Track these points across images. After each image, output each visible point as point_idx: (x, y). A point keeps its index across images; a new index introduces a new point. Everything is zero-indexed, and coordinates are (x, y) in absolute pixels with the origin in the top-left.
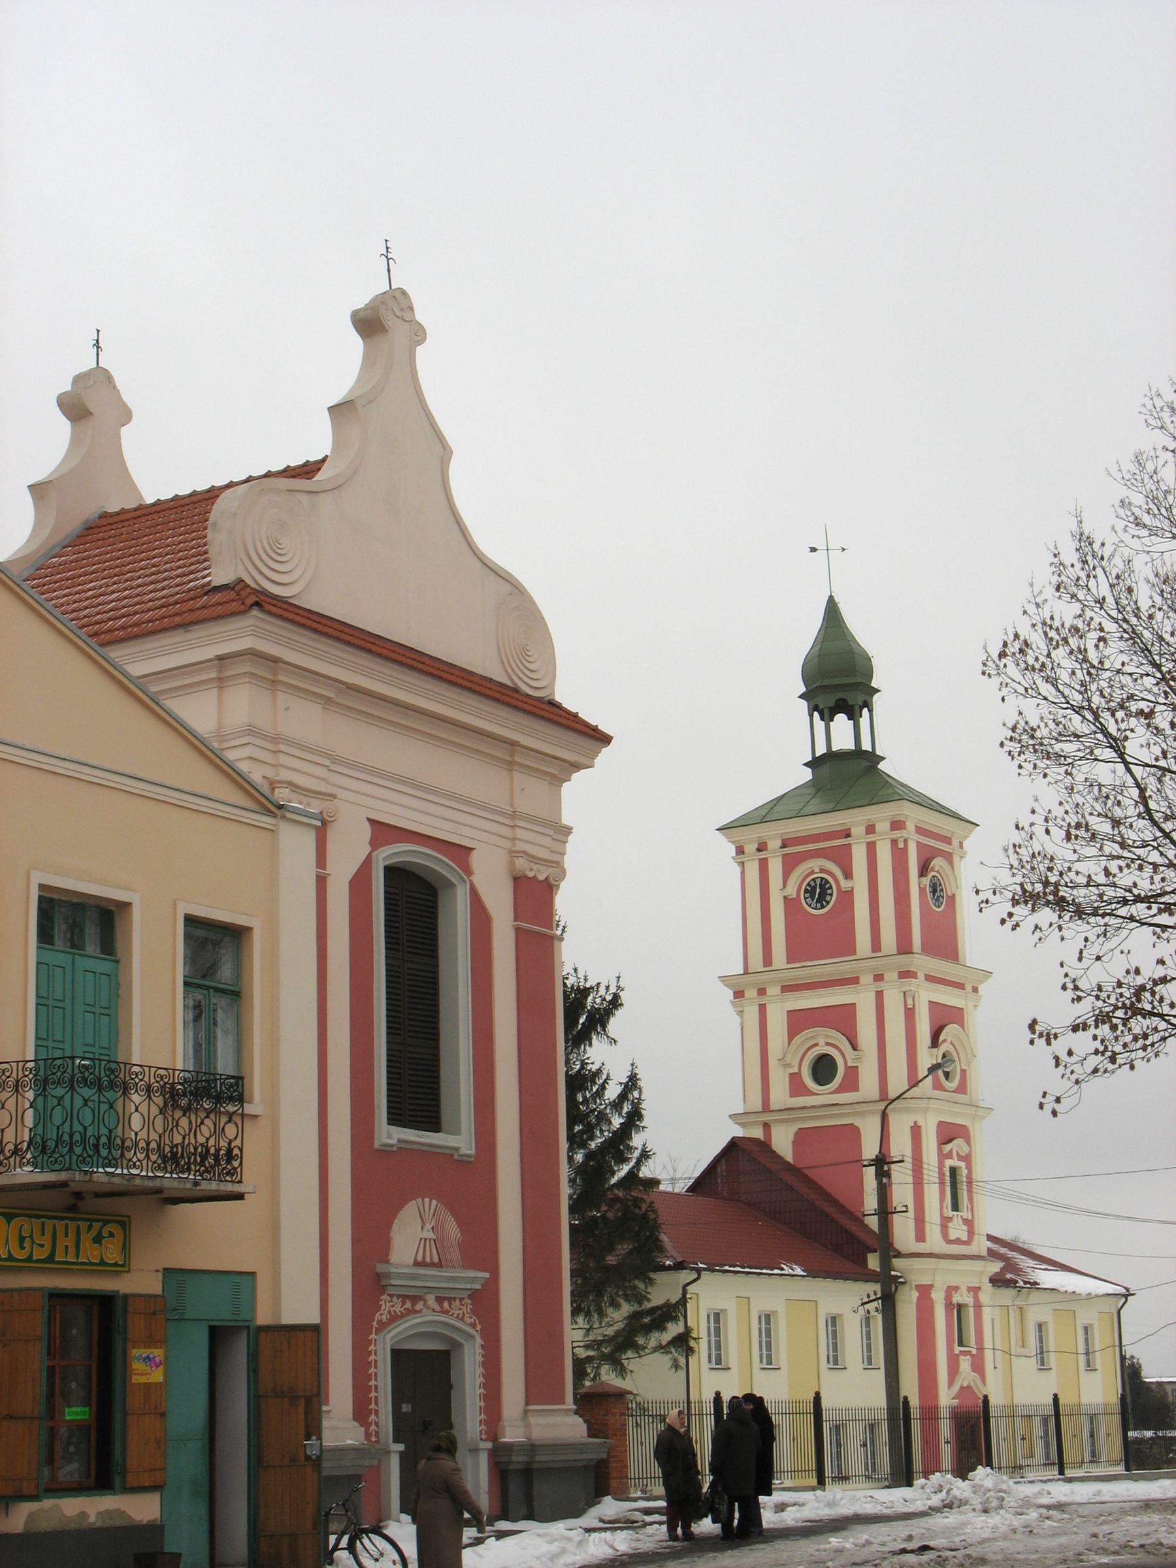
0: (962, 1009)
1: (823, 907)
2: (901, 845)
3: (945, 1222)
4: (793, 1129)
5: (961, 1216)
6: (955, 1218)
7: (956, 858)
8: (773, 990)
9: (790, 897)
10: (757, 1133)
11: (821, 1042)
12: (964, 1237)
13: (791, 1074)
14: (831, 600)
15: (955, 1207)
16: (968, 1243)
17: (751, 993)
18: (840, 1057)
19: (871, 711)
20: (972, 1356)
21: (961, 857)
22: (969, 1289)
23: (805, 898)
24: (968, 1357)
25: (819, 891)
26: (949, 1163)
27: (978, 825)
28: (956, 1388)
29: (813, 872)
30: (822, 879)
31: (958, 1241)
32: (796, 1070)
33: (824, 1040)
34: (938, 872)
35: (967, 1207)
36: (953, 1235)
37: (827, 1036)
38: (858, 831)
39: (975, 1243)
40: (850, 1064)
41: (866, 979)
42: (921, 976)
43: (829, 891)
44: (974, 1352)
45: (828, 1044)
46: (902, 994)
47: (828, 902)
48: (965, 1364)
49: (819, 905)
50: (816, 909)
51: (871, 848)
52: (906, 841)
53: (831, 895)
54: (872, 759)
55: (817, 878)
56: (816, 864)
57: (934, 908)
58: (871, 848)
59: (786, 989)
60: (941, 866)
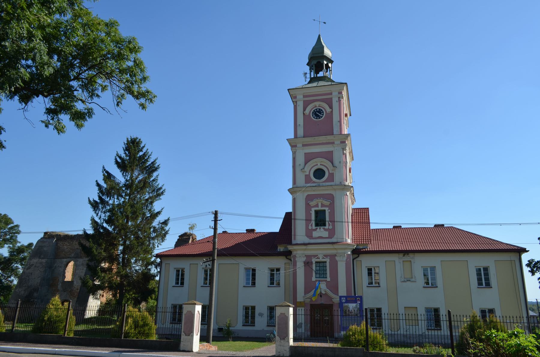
4: (306, 194)
9: (306, 114)
11: (319, 164)
23: (313, 115)
32: (308, 173)
33: (318, 163)
40: (330, 172)
45: (321, 165)
56: (317, 104)
59: (304, 145)
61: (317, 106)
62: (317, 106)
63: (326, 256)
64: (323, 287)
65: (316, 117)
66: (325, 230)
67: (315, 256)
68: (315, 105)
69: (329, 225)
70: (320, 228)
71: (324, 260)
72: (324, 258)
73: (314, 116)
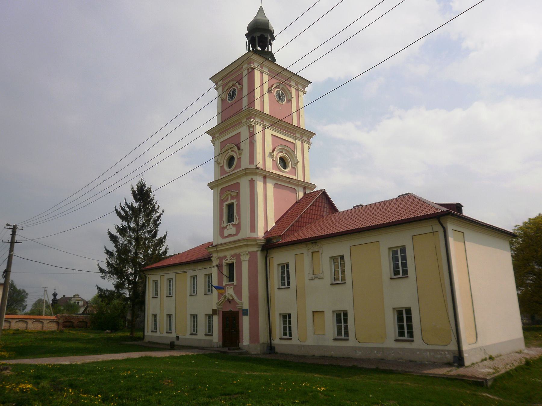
23: (228, 98)
25: (232, 96)
30: (233, 89)
34: (282, 89)
43: (235, 93)
45: (232, 151)
47: (234, 97)
49: (232, 99)
50: (231, 101)
53: (236, 94)
63: (233, 256)
64: (230, 292)
66: (234, 225)
67: (225, 257)
69: (236, 220)
70: (229, 224)
71: (231, 261)
72: (231, 259)
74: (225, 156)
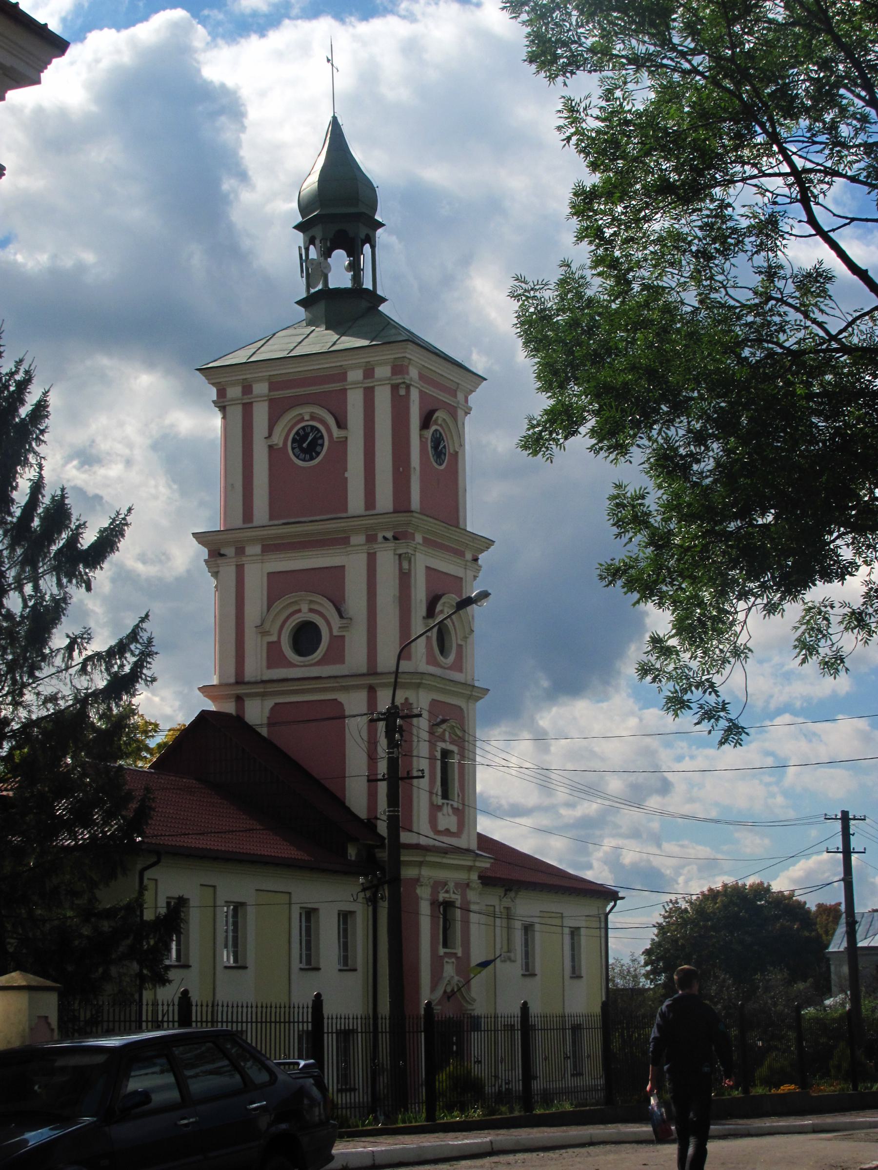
0: (461, 578)
1: (312, 459)
2: (402, 392)
3: (435, 809)
4: (270, 703)
5: (452, 805)
6: (445, 808)
7: (460, 413)
8: (254, 550)
10: (230, 708)
11: (305, 607)
12: (454, 829)
13: (269, 643)
14: (335, 119)
15: (445, 795)
16: (457, 835)
17: (230, 551)
18: (325, 624)
19: (373, 247)
20: (457, 958)
21: (467, 413)
22: (457, 885)
23: (293, 449)
24: (453, 960)
26: (441, 745)
27: (485, 379)
28: (439, 992)
29: (302, 420)
30: (313, 427)
31: (447, 832)
32: (274, 638)
34: (441, 426)
35: (459, 796)
36: (441, 827)
37: (311, 602)
38: (355, 375)
39: (464, 836)
40: (335, 633)
41: (358, 539)
42: (419, 538)
43: (320, 442)
44: (460, 955)
45: (311, 610)
46: (397, 557)
47: (318, 454)
48: (449, 970)
49: (308, 456)
50: (304, 460)
51: (369, 395)
52: (408, 387)
54: (374, 299)
55: (307, 426)
56: (306, 411)
57: (435, 464)
58: (369, 395)
60: (444, 420)
61: (307, 417)
62: (307, 417)
65: (302, 456)
68: (300, 414)
73: (297, 450)
74: (288, 618)
